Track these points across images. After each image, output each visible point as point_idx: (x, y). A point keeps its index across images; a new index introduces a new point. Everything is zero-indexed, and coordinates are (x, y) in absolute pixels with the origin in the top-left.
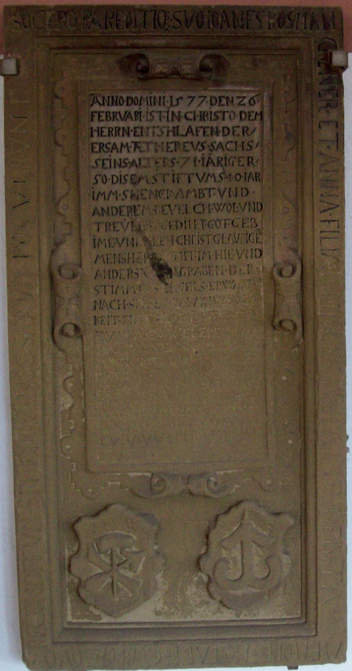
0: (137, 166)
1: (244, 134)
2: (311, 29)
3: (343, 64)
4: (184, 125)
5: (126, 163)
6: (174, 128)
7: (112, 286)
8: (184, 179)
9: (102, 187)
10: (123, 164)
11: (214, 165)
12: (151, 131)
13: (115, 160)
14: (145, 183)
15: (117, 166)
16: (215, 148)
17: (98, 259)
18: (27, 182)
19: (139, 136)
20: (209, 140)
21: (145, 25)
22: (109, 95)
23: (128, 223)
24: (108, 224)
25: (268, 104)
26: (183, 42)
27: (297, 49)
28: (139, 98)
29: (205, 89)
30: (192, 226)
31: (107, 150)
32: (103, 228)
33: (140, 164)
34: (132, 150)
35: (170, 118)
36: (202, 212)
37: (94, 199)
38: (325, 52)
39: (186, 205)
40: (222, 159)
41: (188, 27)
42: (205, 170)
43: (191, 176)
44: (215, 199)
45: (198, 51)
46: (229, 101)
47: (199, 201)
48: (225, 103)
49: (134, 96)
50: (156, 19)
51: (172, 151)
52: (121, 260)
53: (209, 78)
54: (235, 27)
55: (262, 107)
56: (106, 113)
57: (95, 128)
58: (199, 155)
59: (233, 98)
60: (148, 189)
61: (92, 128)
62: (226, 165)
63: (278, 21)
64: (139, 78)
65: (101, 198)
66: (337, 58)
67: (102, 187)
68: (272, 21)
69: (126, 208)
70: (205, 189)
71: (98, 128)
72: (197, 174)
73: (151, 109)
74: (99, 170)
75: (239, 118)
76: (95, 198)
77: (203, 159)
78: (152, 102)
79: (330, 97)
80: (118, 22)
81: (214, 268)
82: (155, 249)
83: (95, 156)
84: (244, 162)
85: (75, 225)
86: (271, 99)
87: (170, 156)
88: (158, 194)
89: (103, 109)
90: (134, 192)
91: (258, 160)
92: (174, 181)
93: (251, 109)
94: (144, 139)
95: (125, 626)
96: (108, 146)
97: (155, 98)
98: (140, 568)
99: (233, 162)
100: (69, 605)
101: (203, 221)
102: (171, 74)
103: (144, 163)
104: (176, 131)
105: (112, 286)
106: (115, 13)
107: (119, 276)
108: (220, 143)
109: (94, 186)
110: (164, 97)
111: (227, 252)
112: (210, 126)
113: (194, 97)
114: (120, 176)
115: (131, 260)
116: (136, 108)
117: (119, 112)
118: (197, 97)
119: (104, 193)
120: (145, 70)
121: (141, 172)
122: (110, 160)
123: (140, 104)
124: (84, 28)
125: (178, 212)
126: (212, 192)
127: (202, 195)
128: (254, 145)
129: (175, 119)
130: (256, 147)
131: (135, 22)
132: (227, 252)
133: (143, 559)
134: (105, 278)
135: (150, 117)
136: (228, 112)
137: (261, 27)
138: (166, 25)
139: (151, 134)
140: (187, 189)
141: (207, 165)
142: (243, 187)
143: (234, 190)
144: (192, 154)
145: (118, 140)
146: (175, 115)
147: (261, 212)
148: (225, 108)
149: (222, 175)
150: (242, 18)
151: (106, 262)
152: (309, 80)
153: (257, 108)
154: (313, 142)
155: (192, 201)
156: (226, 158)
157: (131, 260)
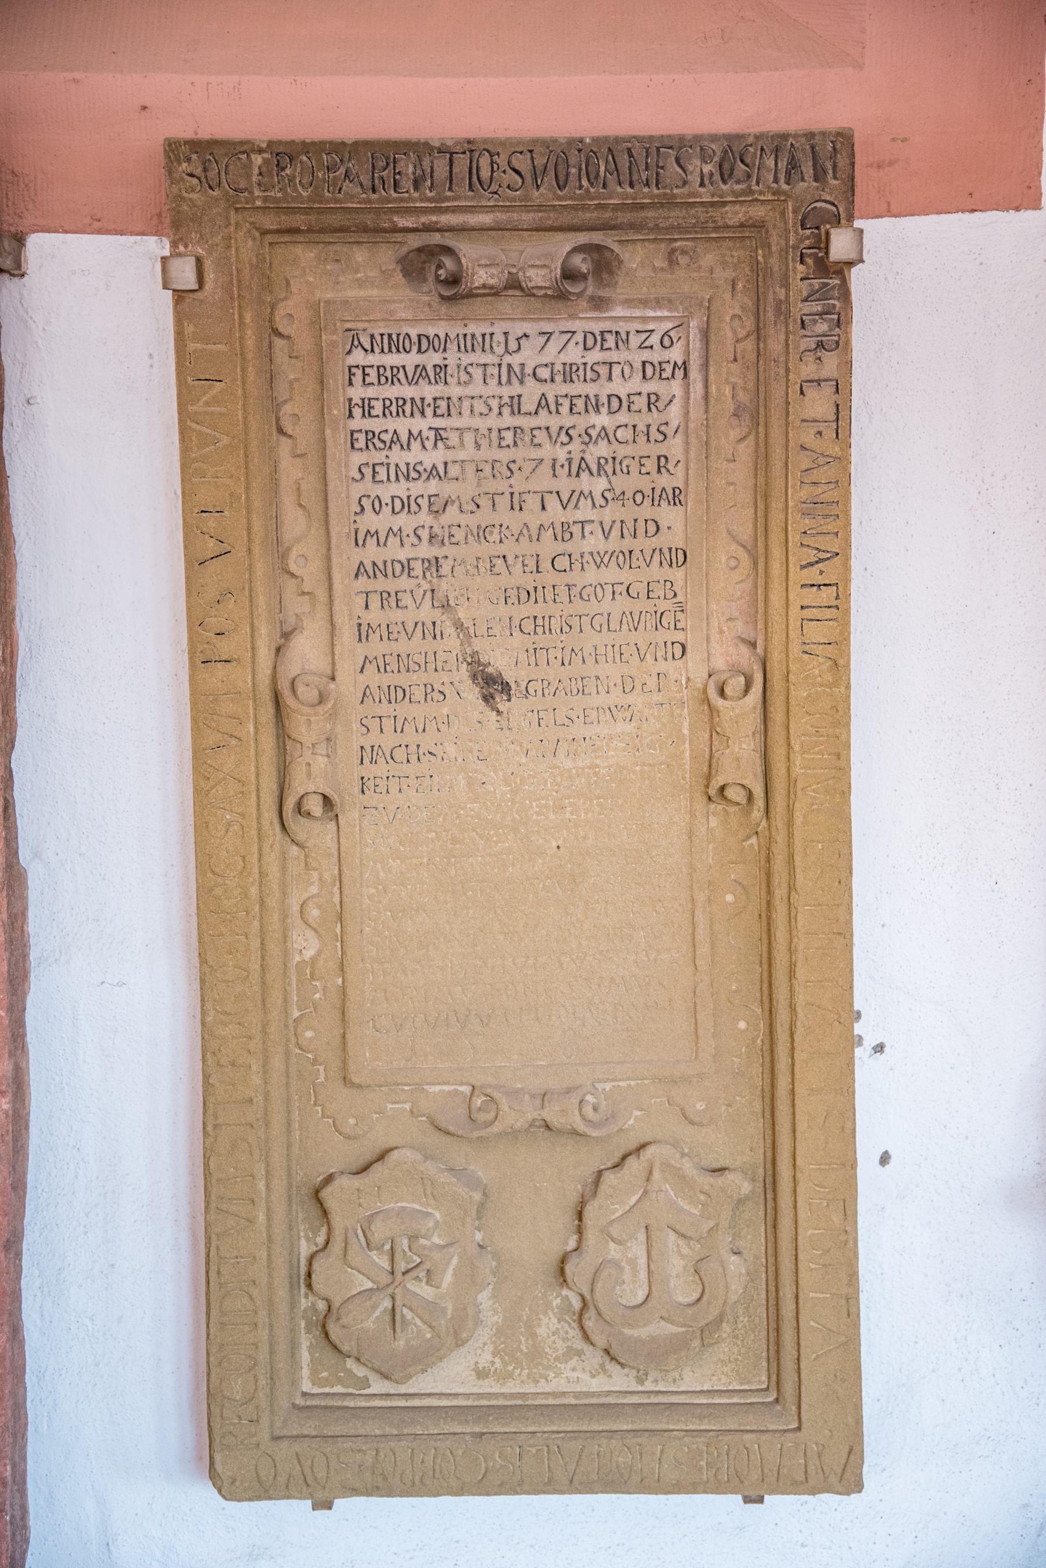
0: (440, 477)
1: (650, 409)
2: (788, 184)
3: (853, 256)
4: (531, 393)
5: (418, 472)
6: (512, 398)
7: (395, 717)
8: (532, 502)
9: (370, 521)
10: (413, 475)
11: (591, 474)
12: (466, 404)
13: (397, 465)
14: (458, 512)
16: (594, 438)
17: (367, 664)
18: (226, 513)
19: (443, 415)
20: (581, 422)
21: (451, 183)
22: (382, 331)
23: (425, 592)
24: (385, 595)
25: (698, 345)
26: (528, 218)
27: (759, 225)
28: (442, 336)
29: (573, 317)
30: (549, 597)
31: (382, 446)
32: (375, 601)
33: (446, 473)
34: (429, 444)
35: (504, 379)
36: (568, 569)
37: (357, 544)
38: (816, 231)
39: (538, 556)
40: (606, 459)
41: (538, 187)
42: (573, 483)
43: (547, 497)
44: (594, 542)
45: (559, 236)
46: (622, 340)
47: (560, 547)
48: (613, 345)
49: (431, 332)
50: (473, 170)
51: (508, 446)
53: (580, 295)
54: (631, 185)
55: (687, 353)
56: (378, 367)
57: (356, 400)
58: (562, 455)
59: (628, 333)
60: (463, 524)
61: (350, 400)
62: (614, 473)
63: (721, 166)
64: (442, 297)
65: (371, 542)
66: (840, 245)
67: (370, 521)
68: (707, 169)
69: (420, 562)
70: (574, 522)
71: (363, 400)
72: (558, 493)
73: (467, 359)
74: (367, 486)
75: (641, 374)
76: (360, 542)
77: (570, 461)
78: (469, 345)
79: (822, 327)
80: (397, 177)
81: (593, 679)
82: (477, 644)
83: (357, 459)
84: (650, 465)
85: (321, 595)
86: (706, 335)
87: (504, 456)
88: (482, 533)
89: (374, 359)
90: (436, 530)
91: (679, 461)
92: (512, 508)
93: (667, 355)
94: (454, 422)
95: (416, 1402)
96: (383, 436)
97: (473, 336)
98: (448, 1278)
99: (627, 466)
100: (305, 1357)
101: (569, 587)
102: (506, 288)
103: (454, 471)
104: (515, 405)
105: (395, 717)
106: (392, 158)
107: (407, 697)
108: (603, 428)
109: (357, 518)
110: (492, 334)
111: (617, 648)
112: (584, 394)
113: (551, 333)
114: (409, 497)
115: (431, 667)
116: (436, 358)
117: (404, 367)
118: (557, 334)
119: (377, 532)
120: (454, 281)
121: (448, 489)
122: (388, 465)
123: (445, 350)
124: (328, 191)
125: (521, 570)
126: (588, 528)
127: (567, 536)
128: (669, 431)
129: (514, 380)
130: (674, 437)
131: (432, 177)
132: (617, 648)
133: (455, 1261)
134: (380, 701)
135: (464, 377)
136: (619, 363)
137: (685, 183)
138: (493, 184)
139: (466, 412)
140: (539, 523)
141: (578, 475)
142: (648, 517)
143: (630, 524)
144: (547, 451)
145: (402, 425)
146: (515, 372)
147: (683, 567)
148: (614, 356)
149: (607, 494)
150: (647, 163)
151: (382, 670)
152: (781, 293)
153: (676, 354)
154: (787, 424)
155: (548, 547)
156: (614, 458)
157: (431, 667)
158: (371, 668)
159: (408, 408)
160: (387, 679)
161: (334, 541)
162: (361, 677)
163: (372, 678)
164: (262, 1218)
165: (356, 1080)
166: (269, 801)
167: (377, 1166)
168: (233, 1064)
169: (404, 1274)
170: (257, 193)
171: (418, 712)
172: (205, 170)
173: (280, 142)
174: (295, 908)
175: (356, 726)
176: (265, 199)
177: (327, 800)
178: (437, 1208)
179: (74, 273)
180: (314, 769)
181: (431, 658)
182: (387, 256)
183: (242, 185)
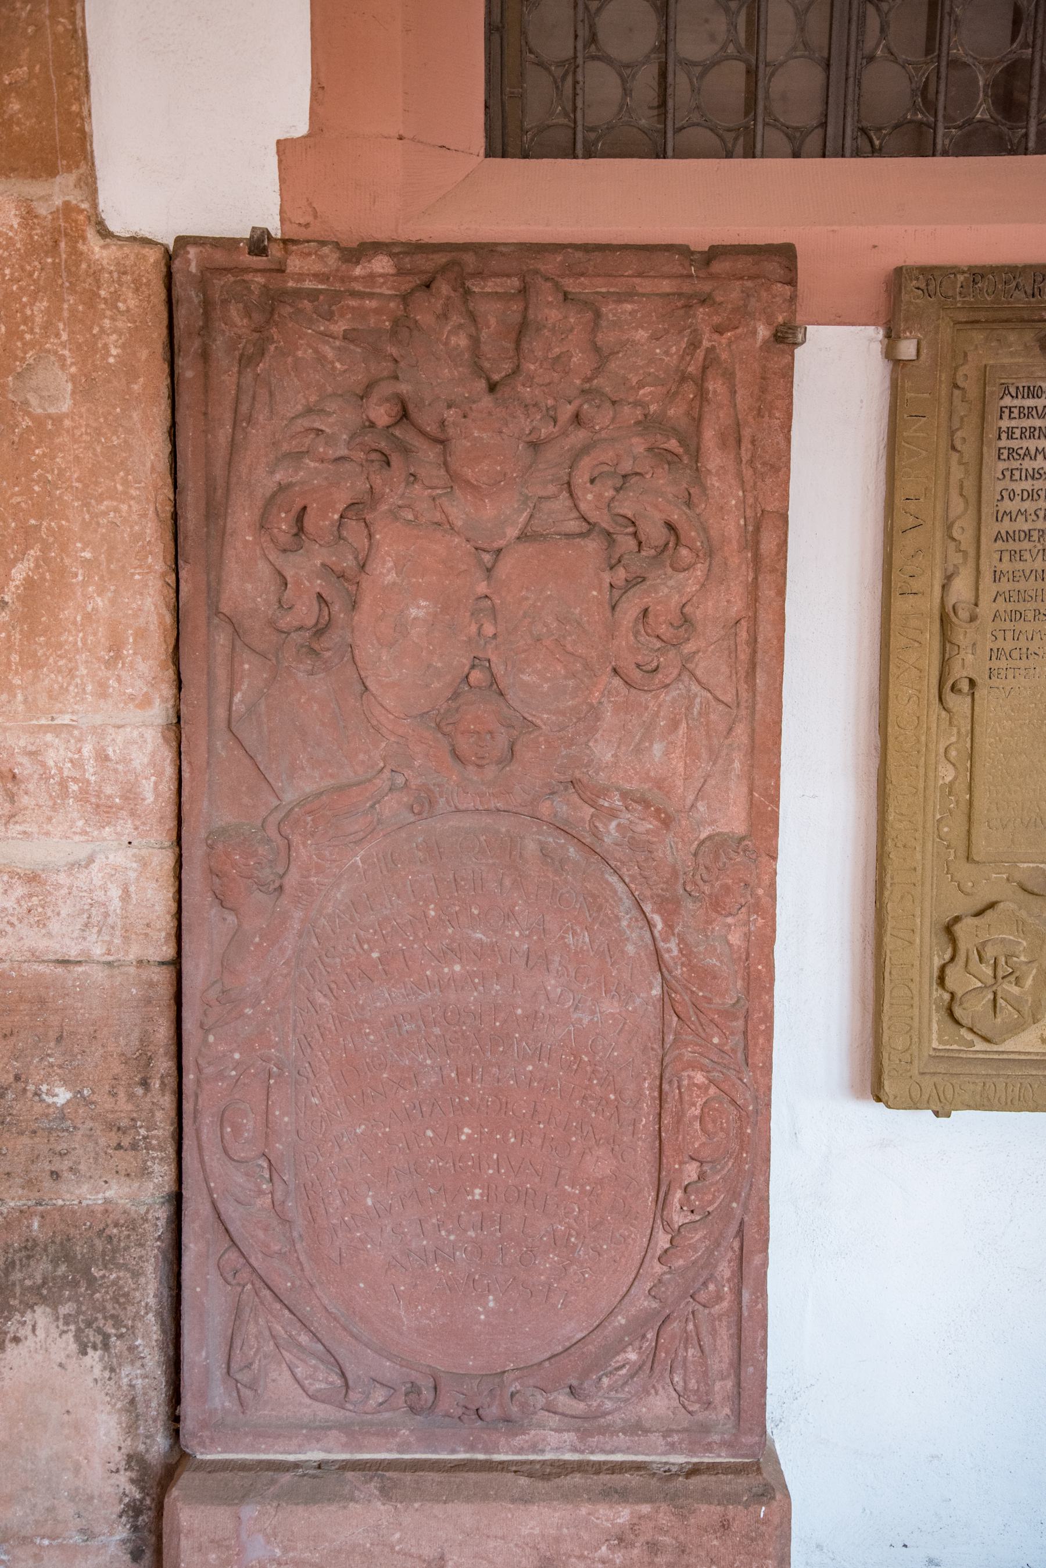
9: (1007, 505)
10: (1037, 476)
15: (1029, 478)
32: (1006, 557)
52: (1028, 598)
57: (1004, 428)
65: (1007, 519)
67: (1007, 505)
74: (1007, 483)
83: (1002, 465)
85: (972, 552)
89: (1017, 402)
95: (1005, 1056)
96: (1019, 451)
98: (1029, 982)
100: (935, 1027)
115: (1039, 598)
133: (1034, 971)
157: (1039, 598)
158: (1000, 599)
159: (1037, 434)
160: (1010, 607)
161: (983, 518)
162: (994, 605)
163: (1001, 605)
164: (918, 941)
165: (976, 858)
166: (935, 681)
167: (990, 912)
168: (904, 846)
169: (1003, 978)
170: (958, 299)
171: (1028, 627)
172: (927, 285)
173: (976, 267)
174: (942, 751)
175: (989, 635)
176: (964, 302)
177: (972, 683)
178: (1024, 939)
179: (821, 350)
180: (967, 662)
181: (1039, 593)
182: (1029, 336)
183: (950, 294)
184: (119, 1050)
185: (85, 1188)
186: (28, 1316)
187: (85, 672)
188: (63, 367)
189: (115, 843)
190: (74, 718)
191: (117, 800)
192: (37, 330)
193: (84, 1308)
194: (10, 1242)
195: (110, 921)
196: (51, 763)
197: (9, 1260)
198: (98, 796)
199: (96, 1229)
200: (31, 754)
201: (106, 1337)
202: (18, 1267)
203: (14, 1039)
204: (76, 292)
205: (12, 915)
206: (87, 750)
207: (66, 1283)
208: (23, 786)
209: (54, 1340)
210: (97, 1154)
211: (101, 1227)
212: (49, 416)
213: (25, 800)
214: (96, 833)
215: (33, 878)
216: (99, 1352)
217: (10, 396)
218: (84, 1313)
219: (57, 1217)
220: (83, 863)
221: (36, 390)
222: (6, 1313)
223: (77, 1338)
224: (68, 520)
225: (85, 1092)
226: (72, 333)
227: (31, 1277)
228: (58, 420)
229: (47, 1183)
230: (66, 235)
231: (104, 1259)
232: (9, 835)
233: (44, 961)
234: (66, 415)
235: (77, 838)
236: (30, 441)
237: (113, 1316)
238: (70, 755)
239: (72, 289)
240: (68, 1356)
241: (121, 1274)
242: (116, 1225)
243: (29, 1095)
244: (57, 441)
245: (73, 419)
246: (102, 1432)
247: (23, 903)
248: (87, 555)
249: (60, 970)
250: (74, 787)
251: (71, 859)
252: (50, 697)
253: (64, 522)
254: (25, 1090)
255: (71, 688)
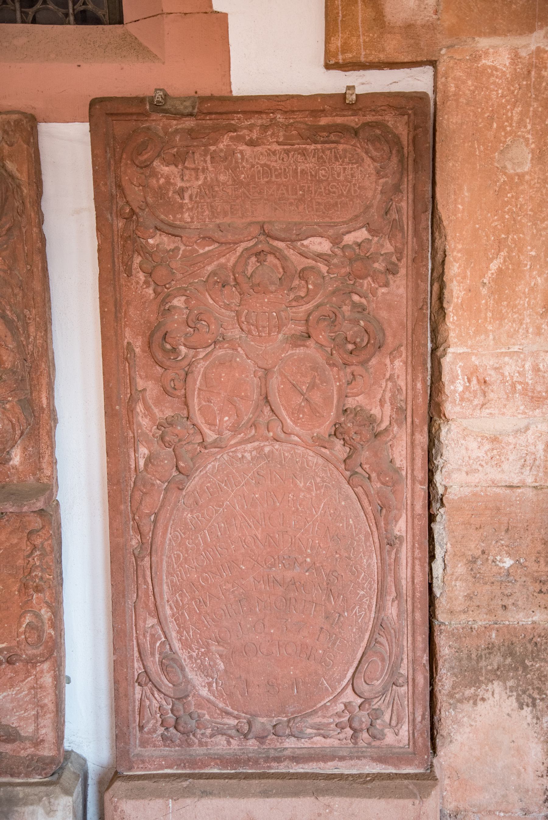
184: (541, 537)
185: (521, 615)
186: (490, 686)
187: (529, 321)
188: (527, 145)
189: (541, 419)
190: (521, 347)
191: (544, 394)
192: (514, 125)
193: (521, 683)
194: (479, 645)
195: (537, 463)
196: (507, 374)
197: (479, 655)
198: (533, 392)
199: (528, 638)
200: (496, 369)
201: (534, 699)
202: (484, 659)
203: (481, 530)
204: (538, 100)
205: (482, 461)
206: (528, 365)
207: (510, 668)
208: (491, 387)
209: (504, 701)
210: (528, 596)
211: (531, 636)
212: (517, 174)
213: (491, 395)
214: (531, 413)
215: (494, 440)
216: (530, 708)
217: (496, 164)
218: (521, 686)
219: (506, 631)
220: (523, 430)
221: (511, 160)
222: (477, 685)
223: (518, 700)
224: (524, 234)
225: (522, 561)
226: (534, 124)
227: (491, 664)
228: (521, 176)
229: (500, 612)
230: (536, 66)
231: (532, 656)
232: (482, 415)
233: (498, 486)
234: (527, 173)
235: (520, 416)
236: (505, 189)
237: (538, 688)
238: (518, 369)
239: (536, 99)
240: (512, 710)
241: (542, 664)
242: (539, 636)
243: (490, 562)
244: (521, 188)
245: (531, 175)
246: (533, 753)
247: (488, 453)
248: (533, 253)
249: (508, 491)
250: (519, 387)
251: (515, 428)
252: (508, 336)
253: (521, 235)
254: (487, 559)
255: (520, 330)
